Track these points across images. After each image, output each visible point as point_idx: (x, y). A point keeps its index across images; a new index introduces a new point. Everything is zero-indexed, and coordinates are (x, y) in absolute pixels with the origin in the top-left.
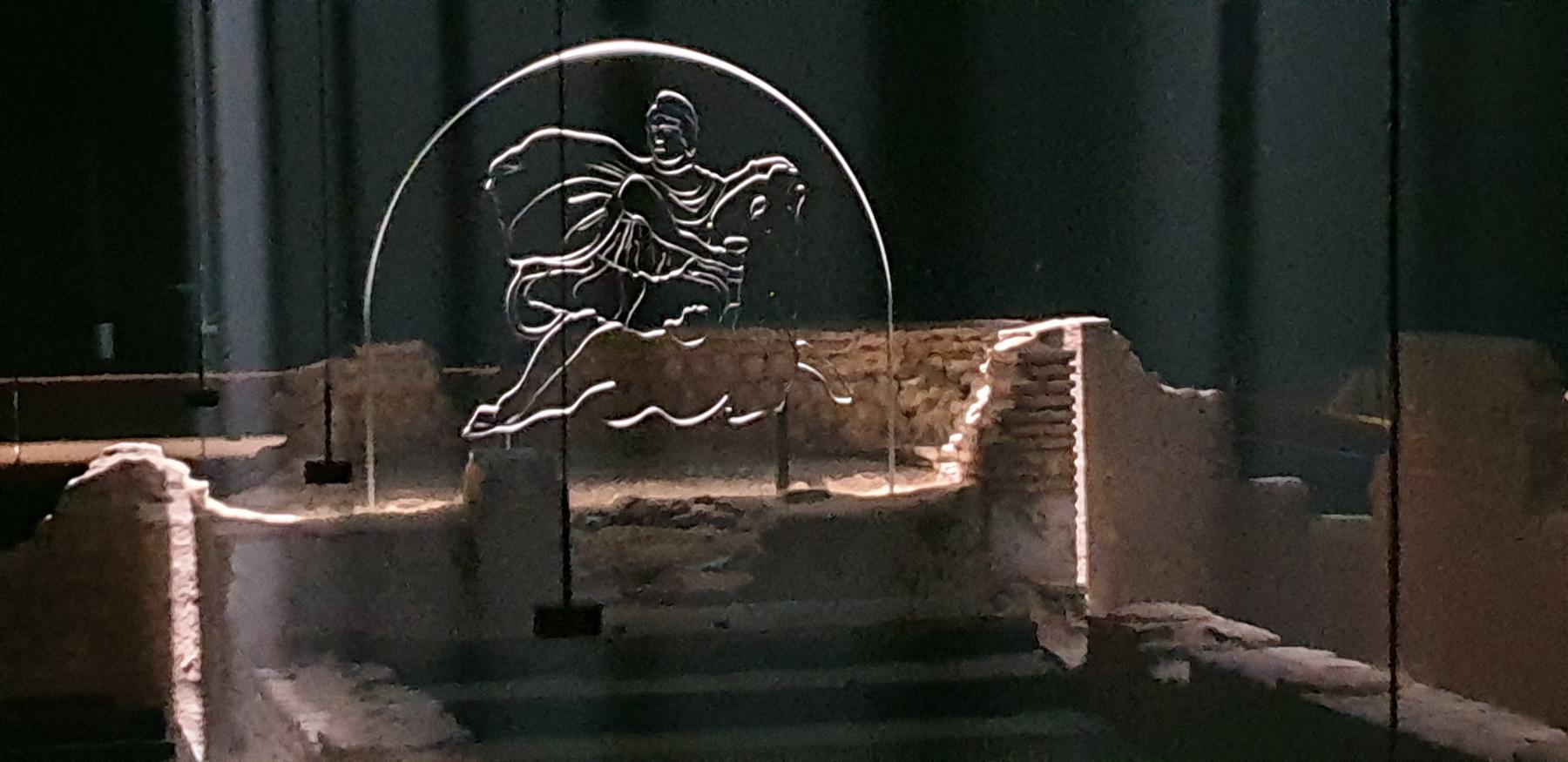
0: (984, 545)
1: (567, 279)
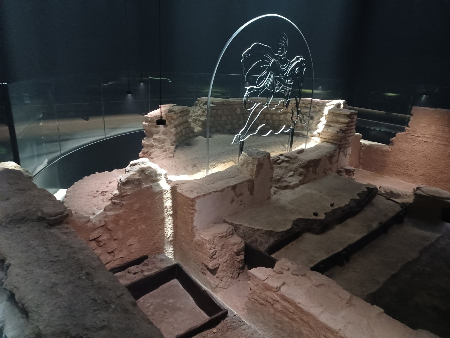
0: (337, 161)
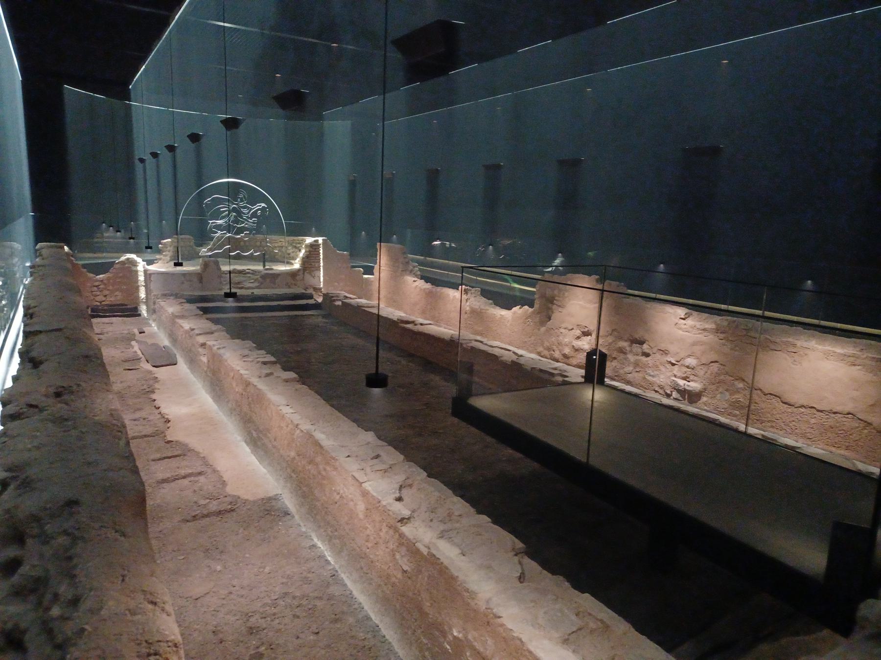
0: (303, 279)
1: (221, 225)
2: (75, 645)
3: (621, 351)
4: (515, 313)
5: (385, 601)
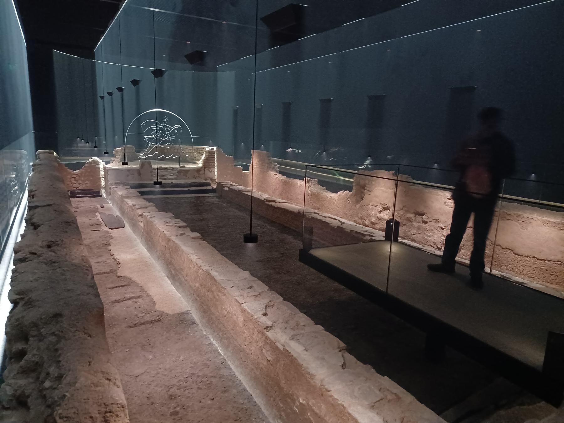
0: (204, 173)
2: (59, 405)
3: (409, 220)
4: (340, 195)
5: (256, 380)
